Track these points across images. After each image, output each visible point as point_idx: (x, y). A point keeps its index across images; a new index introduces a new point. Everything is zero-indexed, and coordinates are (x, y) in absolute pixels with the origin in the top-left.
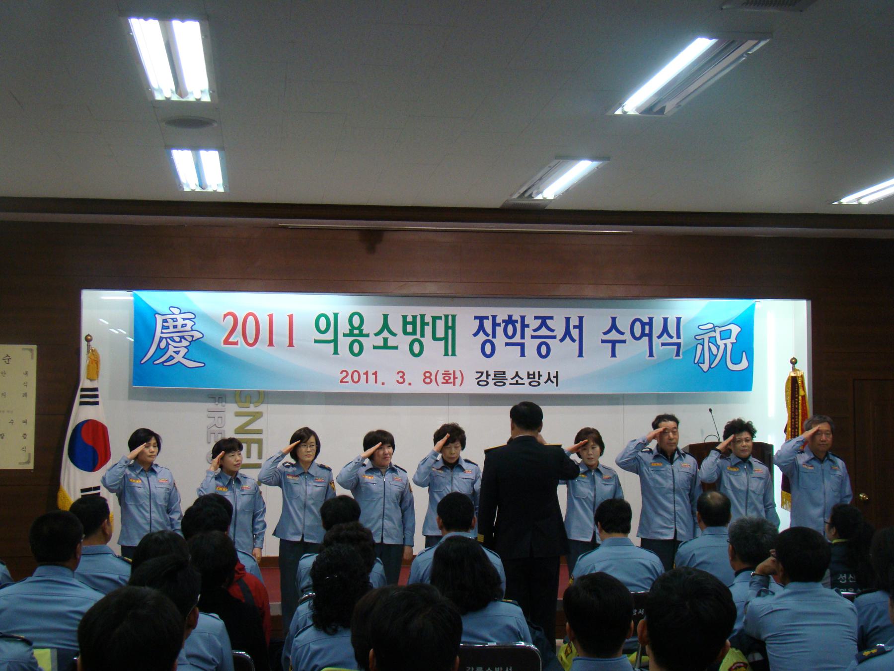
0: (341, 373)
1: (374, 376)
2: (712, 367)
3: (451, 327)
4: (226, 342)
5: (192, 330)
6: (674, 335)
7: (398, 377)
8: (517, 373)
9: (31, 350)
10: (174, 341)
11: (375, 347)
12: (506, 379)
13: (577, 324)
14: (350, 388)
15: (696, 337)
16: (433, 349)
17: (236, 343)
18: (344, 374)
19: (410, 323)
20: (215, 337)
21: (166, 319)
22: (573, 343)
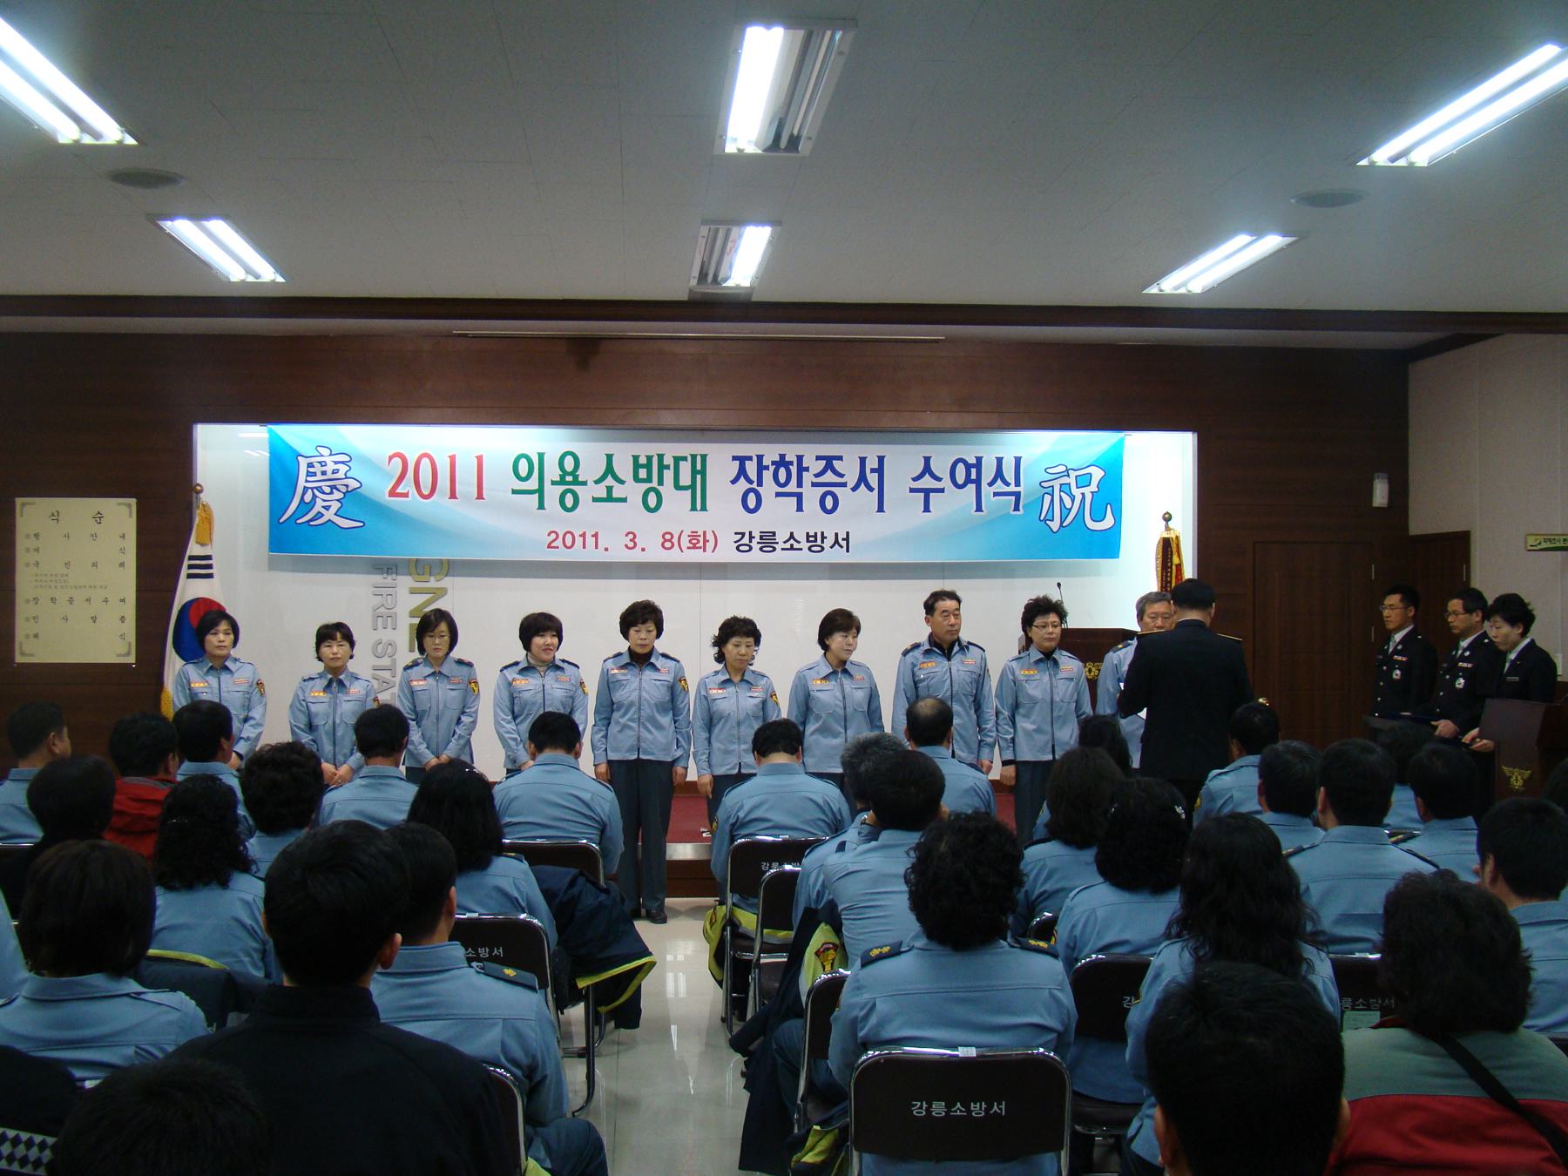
0: (549, 535)
2: (1064, 525)
3: (700, 472)
4: (393, 493)
5: (346, 478)
6: (1011, 480)
7: (627, 540)
8: (792, 534)
9: (129, 506)
10: (324, 493)
11: (595, 500)
12: (777, 543)
13: (876, 466)
14: (561, 555)
15: (1042, 484)
16: (676, 502)
17: (406, 495)
18: (553, 536)
19: (643, 466)
20: (377, 486)
21: (311, 463)
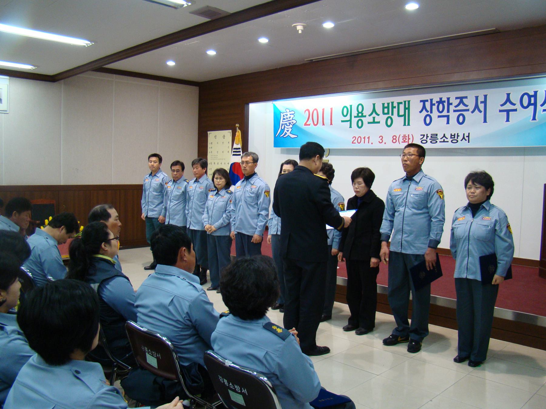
1: (368, 139)
3: (407, 109)
4: (306, 124)
5: (293, 120)
10: (287, 126)
11: (369, 123)
13: (483, 100)
14: (357, 146)
16: (398, 121)
19: (386, 108)
22: (480, 113)
